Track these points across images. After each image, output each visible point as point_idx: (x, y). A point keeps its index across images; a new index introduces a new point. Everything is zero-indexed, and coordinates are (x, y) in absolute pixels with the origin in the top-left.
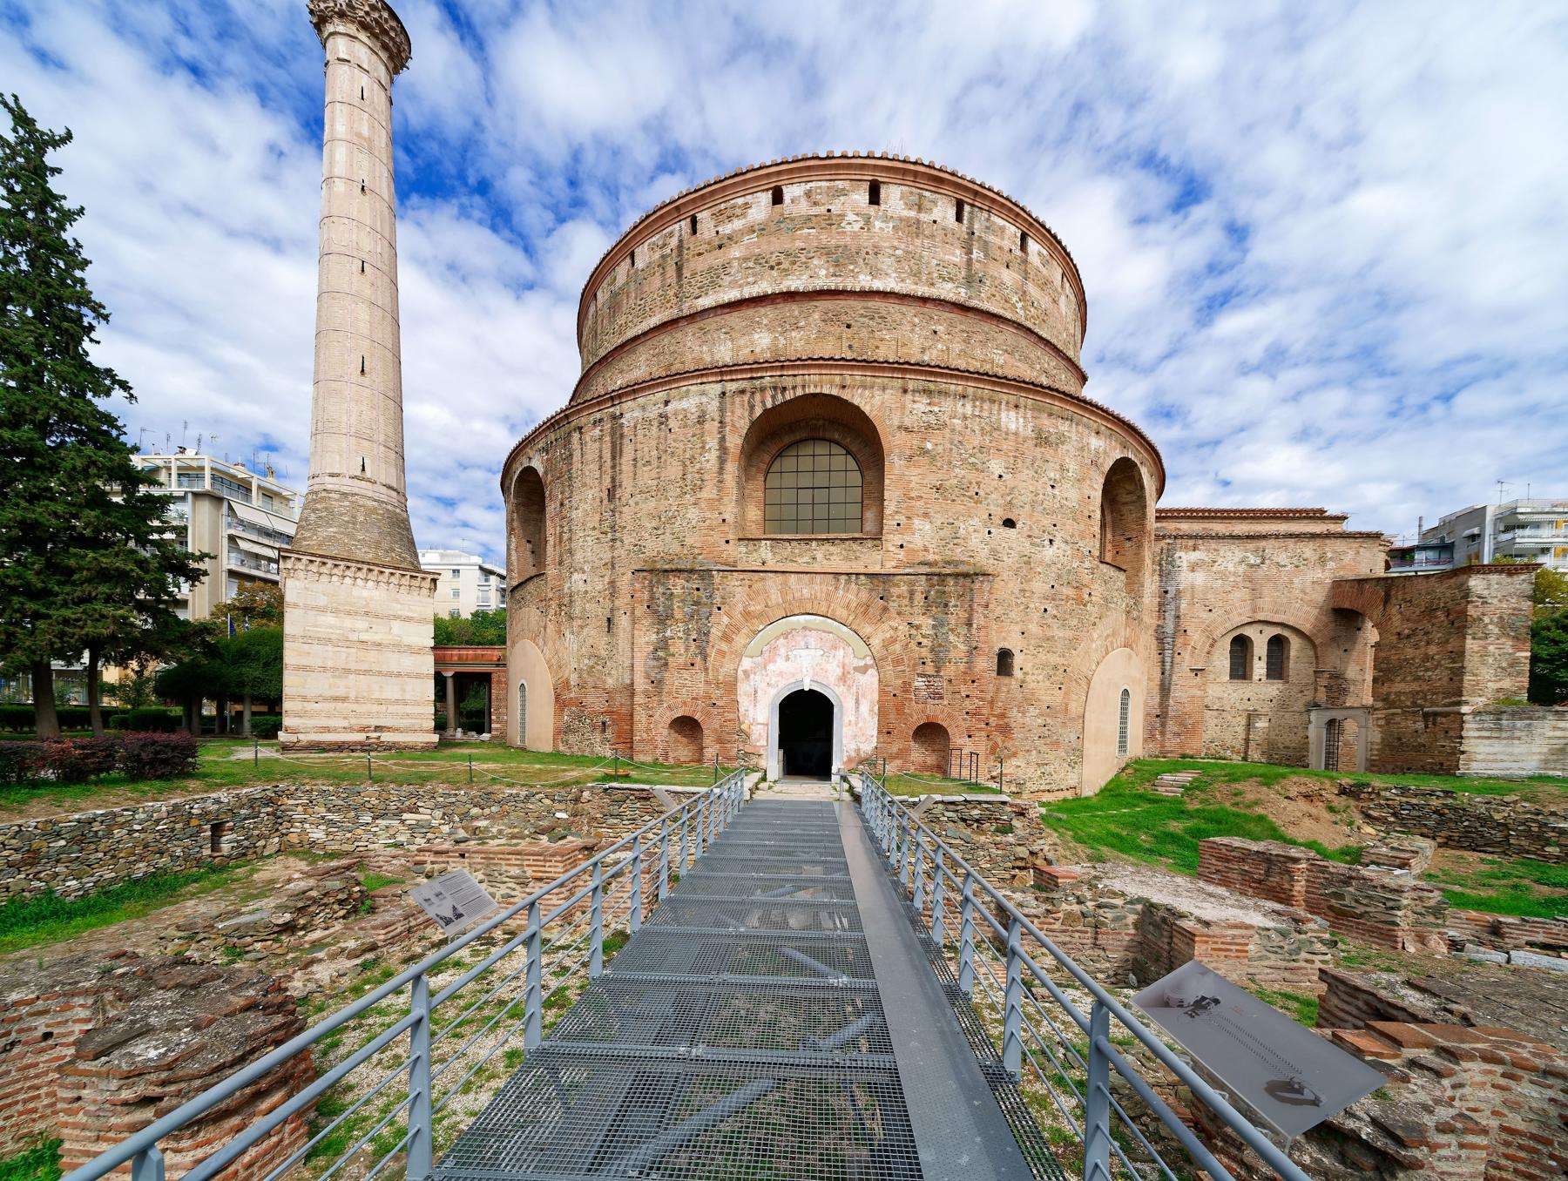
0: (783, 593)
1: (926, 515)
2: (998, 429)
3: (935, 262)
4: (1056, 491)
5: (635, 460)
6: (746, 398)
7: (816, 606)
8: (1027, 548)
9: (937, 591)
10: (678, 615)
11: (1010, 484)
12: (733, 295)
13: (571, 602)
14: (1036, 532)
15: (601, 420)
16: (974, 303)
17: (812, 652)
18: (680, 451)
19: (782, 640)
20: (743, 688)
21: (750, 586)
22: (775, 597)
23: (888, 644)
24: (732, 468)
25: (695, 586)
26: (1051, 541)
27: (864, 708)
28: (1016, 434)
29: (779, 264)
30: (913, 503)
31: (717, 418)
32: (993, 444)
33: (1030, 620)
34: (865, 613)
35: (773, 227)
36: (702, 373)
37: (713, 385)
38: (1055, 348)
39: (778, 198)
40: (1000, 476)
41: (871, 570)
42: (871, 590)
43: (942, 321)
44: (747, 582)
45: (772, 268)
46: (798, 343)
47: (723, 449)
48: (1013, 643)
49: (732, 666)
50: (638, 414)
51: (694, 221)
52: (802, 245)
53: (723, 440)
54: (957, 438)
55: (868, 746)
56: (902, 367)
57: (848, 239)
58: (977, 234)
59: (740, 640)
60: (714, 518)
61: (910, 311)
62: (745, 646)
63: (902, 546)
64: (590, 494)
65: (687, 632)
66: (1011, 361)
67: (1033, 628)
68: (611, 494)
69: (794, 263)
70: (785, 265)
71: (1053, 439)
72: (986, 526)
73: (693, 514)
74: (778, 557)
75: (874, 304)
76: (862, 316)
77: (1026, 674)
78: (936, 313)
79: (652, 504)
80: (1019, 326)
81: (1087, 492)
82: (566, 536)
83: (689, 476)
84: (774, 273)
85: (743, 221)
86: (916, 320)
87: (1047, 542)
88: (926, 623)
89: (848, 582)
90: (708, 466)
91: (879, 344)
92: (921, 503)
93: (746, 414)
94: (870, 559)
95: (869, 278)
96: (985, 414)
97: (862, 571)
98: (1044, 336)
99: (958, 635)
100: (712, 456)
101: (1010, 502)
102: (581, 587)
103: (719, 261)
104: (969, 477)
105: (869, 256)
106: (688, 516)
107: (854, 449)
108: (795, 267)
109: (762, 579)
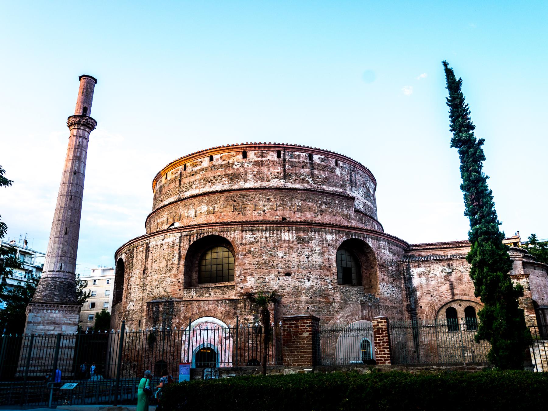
0: (199, 309)
1: (252, 275)
2: (281, 240)
3: (269, 173)
4: (310, 259)
5: (152, 259)
7: (210, 314)
10: (161, 319)
11: (287, 259)
15: (143, 244)
18: (166, 257)
21: (187, 307)
22: (196, 310)
25: (167, 308)
29: (212, 180)
32: (279, 245)
34: (228, 315)
35: (210, 168)
40: (283, 257)
42: (230, 306)
44: (186, 305)
45: (209, 182)
50: (154, 243)
57: (236, 171)
58: (287, 160)
60: (176, 281)
63: (242, 288)
69: (217, 180)
72: (277, 277)
73: (169, 280)
75: (243, 192)
76: (239, 197)
83: (169, 266)
84: (210, 184)
89: (222, 303)
91: (246, 206)
92: (249, 271)
94: (232, 295)
97: (227, 298)
100: (176, 258)
103: (193, 180)
104: (269, 259)
105: (243, 176)
108: (217, 181)
109: (191, 304)
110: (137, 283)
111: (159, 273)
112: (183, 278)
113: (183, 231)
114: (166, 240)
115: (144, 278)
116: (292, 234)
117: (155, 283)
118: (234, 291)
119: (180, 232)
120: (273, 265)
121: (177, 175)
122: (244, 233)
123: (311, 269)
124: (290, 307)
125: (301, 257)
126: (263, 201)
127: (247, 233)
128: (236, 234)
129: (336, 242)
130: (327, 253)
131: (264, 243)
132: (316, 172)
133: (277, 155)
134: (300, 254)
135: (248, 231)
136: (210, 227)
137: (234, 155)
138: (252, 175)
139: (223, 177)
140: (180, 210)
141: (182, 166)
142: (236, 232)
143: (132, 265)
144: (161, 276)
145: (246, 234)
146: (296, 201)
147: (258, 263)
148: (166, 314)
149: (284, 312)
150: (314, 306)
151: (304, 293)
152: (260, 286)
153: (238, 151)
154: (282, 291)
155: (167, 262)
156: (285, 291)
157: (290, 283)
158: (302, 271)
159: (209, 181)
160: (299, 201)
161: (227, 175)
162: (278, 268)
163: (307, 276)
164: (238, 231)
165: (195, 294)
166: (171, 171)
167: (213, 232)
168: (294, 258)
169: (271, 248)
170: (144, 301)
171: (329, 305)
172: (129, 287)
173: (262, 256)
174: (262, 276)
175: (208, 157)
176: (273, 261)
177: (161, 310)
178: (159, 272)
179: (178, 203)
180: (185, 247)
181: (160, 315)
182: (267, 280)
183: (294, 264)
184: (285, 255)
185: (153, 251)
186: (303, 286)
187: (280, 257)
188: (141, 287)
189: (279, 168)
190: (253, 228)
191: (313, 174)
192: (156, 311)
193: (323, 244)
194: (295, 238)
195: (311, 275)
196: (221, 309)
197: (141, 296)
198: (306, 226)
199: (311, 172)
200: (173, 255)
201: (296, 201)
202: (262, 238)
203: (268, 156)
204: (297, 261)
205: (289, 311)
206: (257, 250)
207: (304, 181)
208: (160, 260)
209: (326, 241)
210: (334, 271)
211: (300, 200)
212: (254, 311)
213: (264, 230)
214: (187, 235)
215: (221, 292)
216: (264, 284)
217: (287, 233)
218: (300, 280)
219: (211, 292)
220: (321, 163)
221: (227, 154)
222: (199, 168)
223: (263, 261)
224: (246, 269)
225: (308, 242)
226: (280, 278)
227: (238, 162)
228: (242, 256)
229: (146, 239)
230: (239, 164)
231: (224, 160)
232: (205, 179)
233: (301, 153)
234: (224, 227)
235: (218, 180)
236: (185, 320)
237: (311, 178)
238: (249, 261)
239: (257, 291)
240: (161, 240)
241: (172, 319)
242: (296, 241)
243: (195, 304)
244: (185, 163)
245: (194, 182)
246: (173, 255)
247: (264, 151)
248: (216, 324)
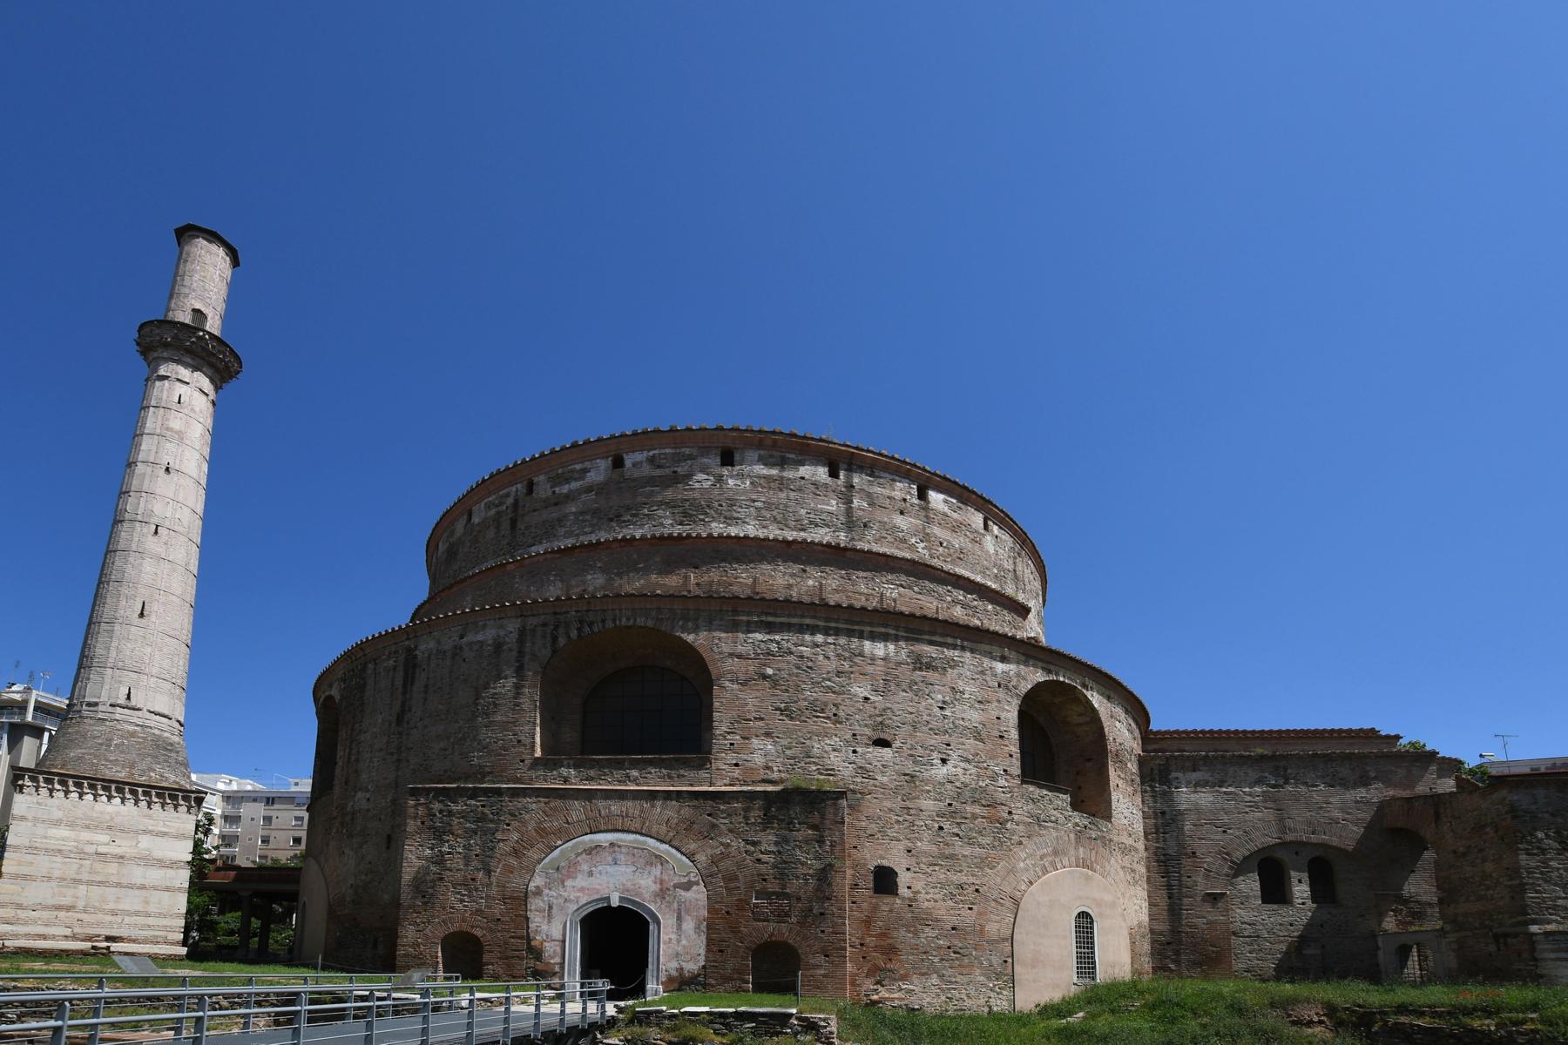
8: (910, 767)
23: (714, 861)
62: (540, 861)
63: (736, 765)
82: (353, 758)
85: (581, 482)
101: (881, 723)
121: (504, 508)
126: (785, 574)
132: (936, 530)
133: (829, 471)
137: (692, 455)
151: (929, 791)
159: (611, 516)
160: (892, 586)
189: (834, 502)
191: (928, 534)
195: (951, 750)
199: (924, 528)
201: (886, 586)
207: (906, 546)
210: (1012, 748)
211: (897, 585)
222: (574, 485)
226: (858, 749)
232: (595, 512)
237: (922, 541)
239: (783, 775)
244: (529, 477)
245: (559, 520)
247: (788, 455)
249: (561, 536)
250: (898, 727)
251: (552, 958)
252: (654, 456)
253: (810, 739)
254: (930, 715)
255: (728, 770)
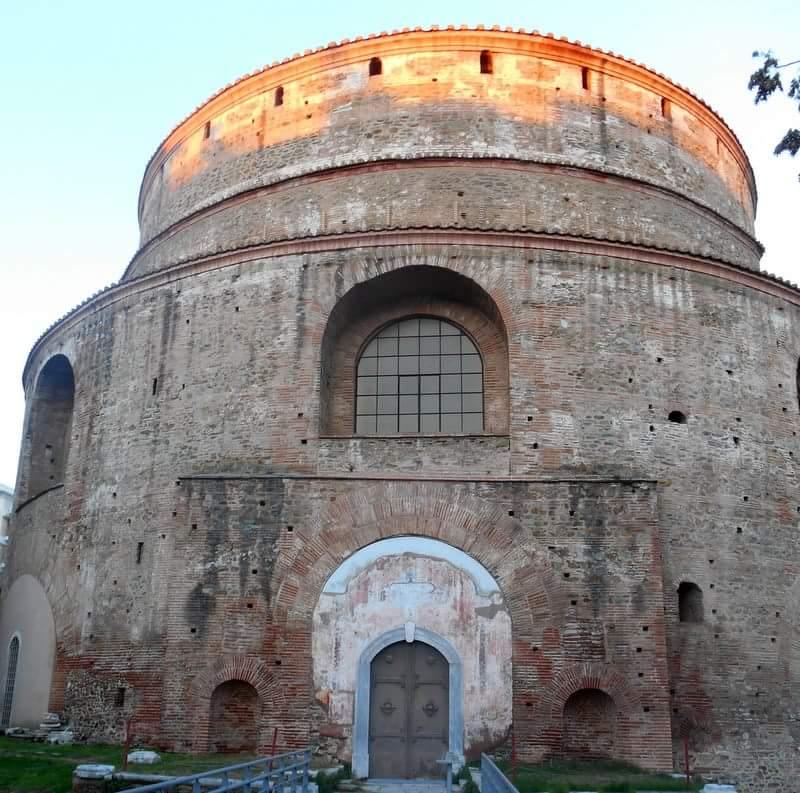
0: (378, 508)
2: (651, 304)
3: (561, 129)
4: (735, 378)
6: (333, 270)
9: (587, 505)
12: (324, 163)
13: (93, 521)
14: (714, 429)
15: (152, 299)
16: (611, 168)
17: (418, 588)
19: (375, 571)
20: (320, 640)
21: (333, 499)
22: (367, 512)
23: (521, 575)
24: (312, 352)
25: (258, 499)
26: (736, 440)
27: (494, 667)
28: (675, 310)
29: (378, 132)
30: (548, 392)
31: (296, 295)
32: (647, 322)
33: (720, 544)
34: (490, 533)
36: (278, 244)
37: (294, 258)
38: (717, 216)
39: (376, 67)
40: (659, 360)
41: (495, 476)
42: (497, 503)
43: (576, 189)
44: (329, 494)
46: (400, 211)
47: (302, 330)
48: (699, 575)
49: (304, 608)
50: (199, 290)
51: (280, 92)
52: (404, 113)
53: (302, 319)
54: (599, 315)
55: (499, 726)
56: (527, 235)
59: (316, 571)
60: (290, 411)
61: (535, 177)
62: (325, 580)
63: (535, 446)
64: (131, 385)
65: (244, 563)
66: (664, 230)
67: (725, 555)
68: (156, 386)
69: (395, 130)
70: (385, 132)
71: (723, 316)
72: (647, 421)
73: (260, 409)
74: (370, 462)
76: (477, 183)
77: (722, 618)
78: (566, 179)
79: (209, 396)
80: (669, 192)
81: (777, 379)
83: (258, 363)
85: (339, 91)
86: (543, 187)
87: (731, 442)
88: (578, 548)
89: (467, 491)
90: (283, 349)
93: (333, 290)
94: (498, 465)
95: (484, 144)
96: (633, 288)
97: (483, 476)
98: (703, 202)
99: (620, 562)
100: (289, 337)
101: (676, 391)
102: (109, 502)
104: (618, 360)
106: (255, 410)
107: (471, 327)
108: (396, 135)
109: (349, 489)
110: (127, 424)
111: (219, 386)
112: (318, 402)
113: (312, 249)
114: (245, 280)
115: (158, 406)
116: (684, 292)
117: (203, 422)
118: (509, 454)
119: (302, 253)
120: (630, 380)
122: (535, 268)
123: (740, 409)
124: (688, 523)
125: (713, 367)
127: (544, 270)
128: (507, 268)
129: (793, 339)
130: (776, 367)
131: (602, 309)
134: (708, 357)
135: (548, 263)
136: (414, 241)
138: (511, 125)
139: (415, 122)
140: (268, 215)
141: (267, 95)
142: (508, 262)
143: (108, 368)
144: (228, 394)
145: (542, 273)
146: (643, 219)
147: (583, 370)
148: (256, 519)
149: (672, 536)
150: (755, 525)
152: (591, 446)
153: (466, 48)
154: (665, 467)
155: (253, 349)
156: (671, 468)
157: (687, 445)
158: (717, 411)
161: (430, 119)
162: (647, 394)
163: (731, 429)
164: (514, 259)
165: (360, 458)
166: (226, 114)
167: (426, 257)
168: (693, 369)
169: (622, 326)
170: (157, 478)
171: (790, 526)
172: (95, 438)
173: (599, 348)
174: (600, 414)
175: (365, 61)
176: (632, 368)
177: (235, 504)
178: (219, 383)
179: (259, 195)
180: (321, 301)
181: (232, 523)
182: (615, 427)
183: (694, 387)
184: (666, 353)
185: (194, 316)
186: (722, 459)
187: (654, 360)
188: (147, 433)
190: (562, 256)
192: (216, 509)
193: (765, 337)
194: (692, 305)
196: (464, 510)
197: (146, 462)
198: (722, 275)
200: (277, 328)
202: (594, 291)
203: (558, 78)
204: (703, 379)
205: (687, 535)
206: (578, 328)
208: (224, 344)
209: (772, 329)
212: (588, 525)
213: (599, 266)
214: (328, 264)
215: (458, 454)
216: (608, 439)
217: (668, 288)
218: (716, 438)
219: (420, 454)
220: (690, 133)
221: (429, 55)
223: (601, 366)
224: (546, 386)
225: (729, 322)
226: (656, 426)
227: (467, 83)
228: (531, 343)
229: (165, 280)
230: (470, 87)
231: (419, 73)
233: (643, 90)
234: (468, 242)
235: (400, 132)
236: (328, 545)
238: (556, 360)
239: (583, 460)
240: (229, 281)
241: (277, 537)
242: (696, 316)
243: (366, 493)
246: (274, 325)
248: (444, 563)
249: (314, 155)
250: (691, 397)
251: (341, 717)
252: (412, 61)
253: (608, 411)
254: (720, 382)
255: (527, 453)
